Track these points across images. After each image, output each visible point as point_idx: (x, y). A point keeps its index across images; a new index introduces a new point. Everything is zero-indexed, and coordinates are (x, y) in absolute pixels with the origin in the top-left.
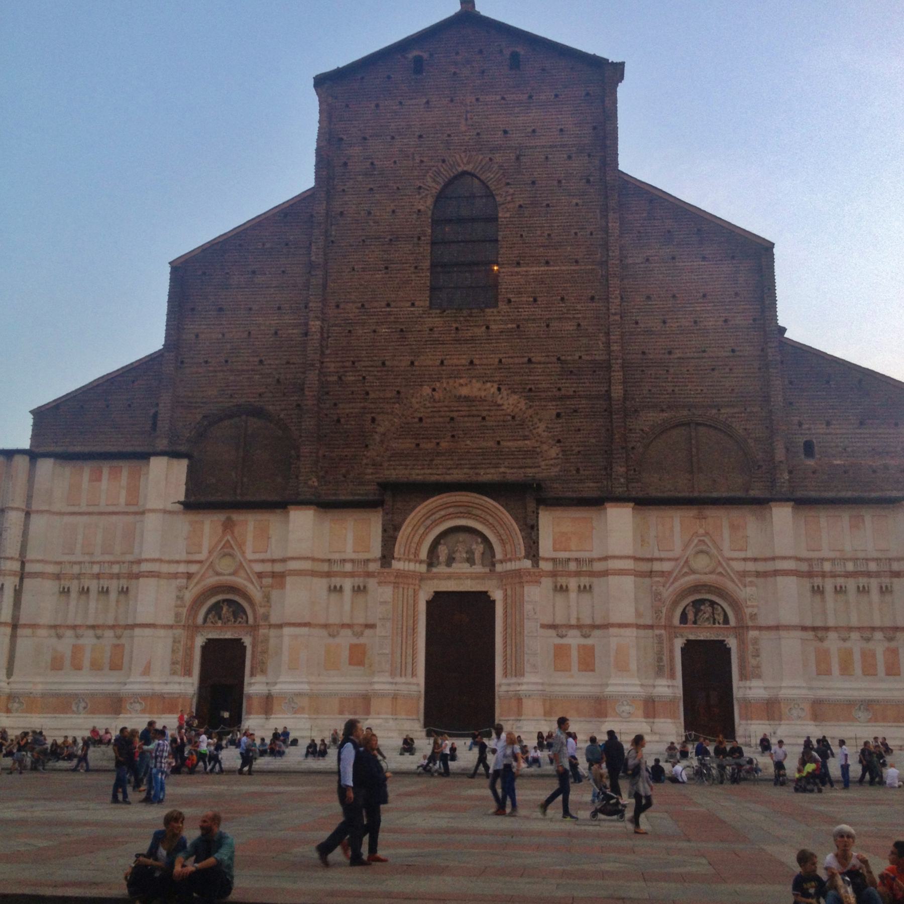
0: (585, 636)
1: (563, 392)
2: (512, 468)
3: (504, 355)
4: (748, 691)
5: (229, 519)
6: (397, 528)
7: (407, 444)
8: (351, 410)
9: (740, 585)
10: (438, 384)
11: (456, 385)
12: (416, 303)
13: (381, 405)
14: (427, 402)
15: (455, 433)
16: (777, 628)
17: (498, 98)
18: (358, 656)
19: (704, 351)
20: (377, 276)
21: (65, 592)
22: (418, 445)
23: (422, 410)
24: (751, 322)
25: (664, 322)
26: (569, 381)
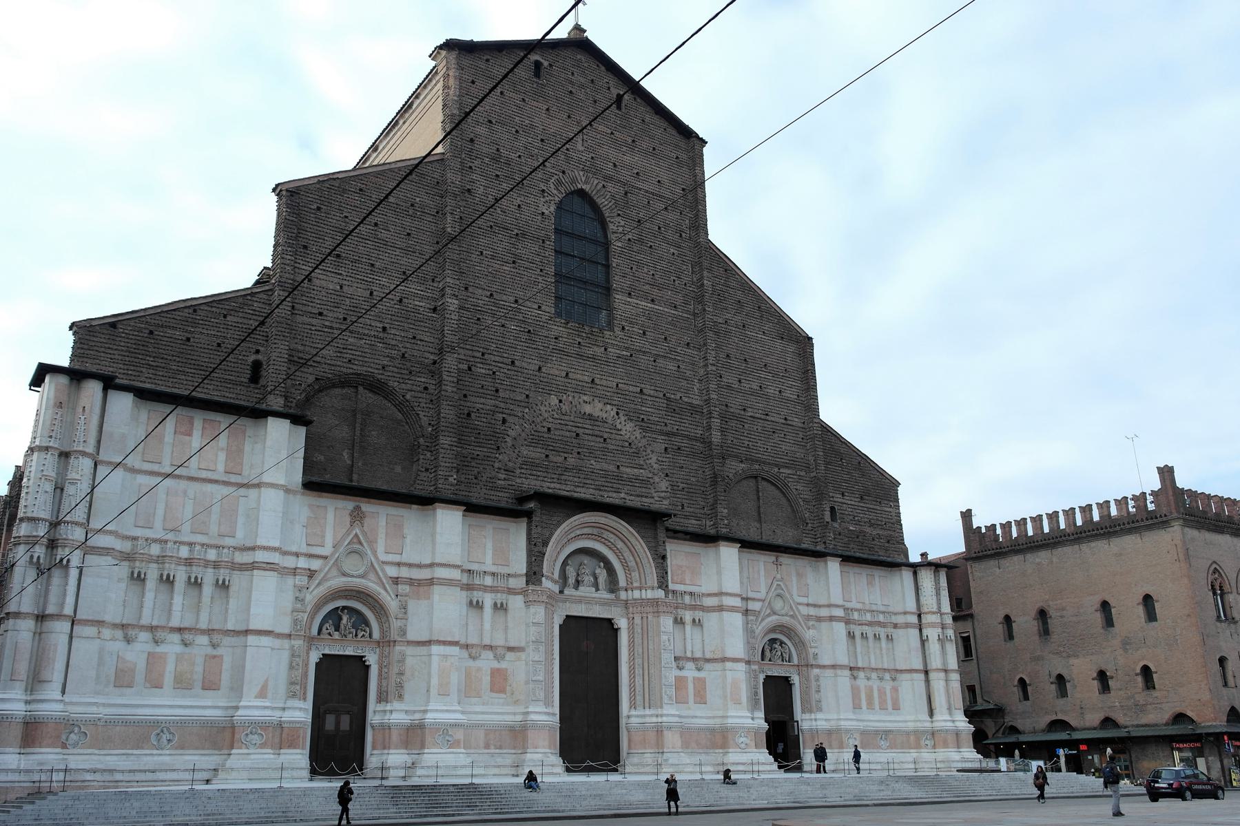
0: (699, 669)
1: (669, 428)
2: (631, 495)
3: (621, 381)
4: (814, 723)
5: (358, 508)
6: (546, 544)
7: (536, 454)
8: (481, 406)
9: (805, 627)
10: (565, 396)
11: (581, 401)
12: (543, 308)
13: (512, 407)
14: (555, 413)
15: (580, 450)
16: (834, 667)
17: (609, 131)
18: (499, 682)
19: (767, 415)
20: (506, 268)
21: (138, 579)
22: (547, 456)
23: (551, 420)
24: (796, 397)
25: (740, 381)
26: (673, 419)
